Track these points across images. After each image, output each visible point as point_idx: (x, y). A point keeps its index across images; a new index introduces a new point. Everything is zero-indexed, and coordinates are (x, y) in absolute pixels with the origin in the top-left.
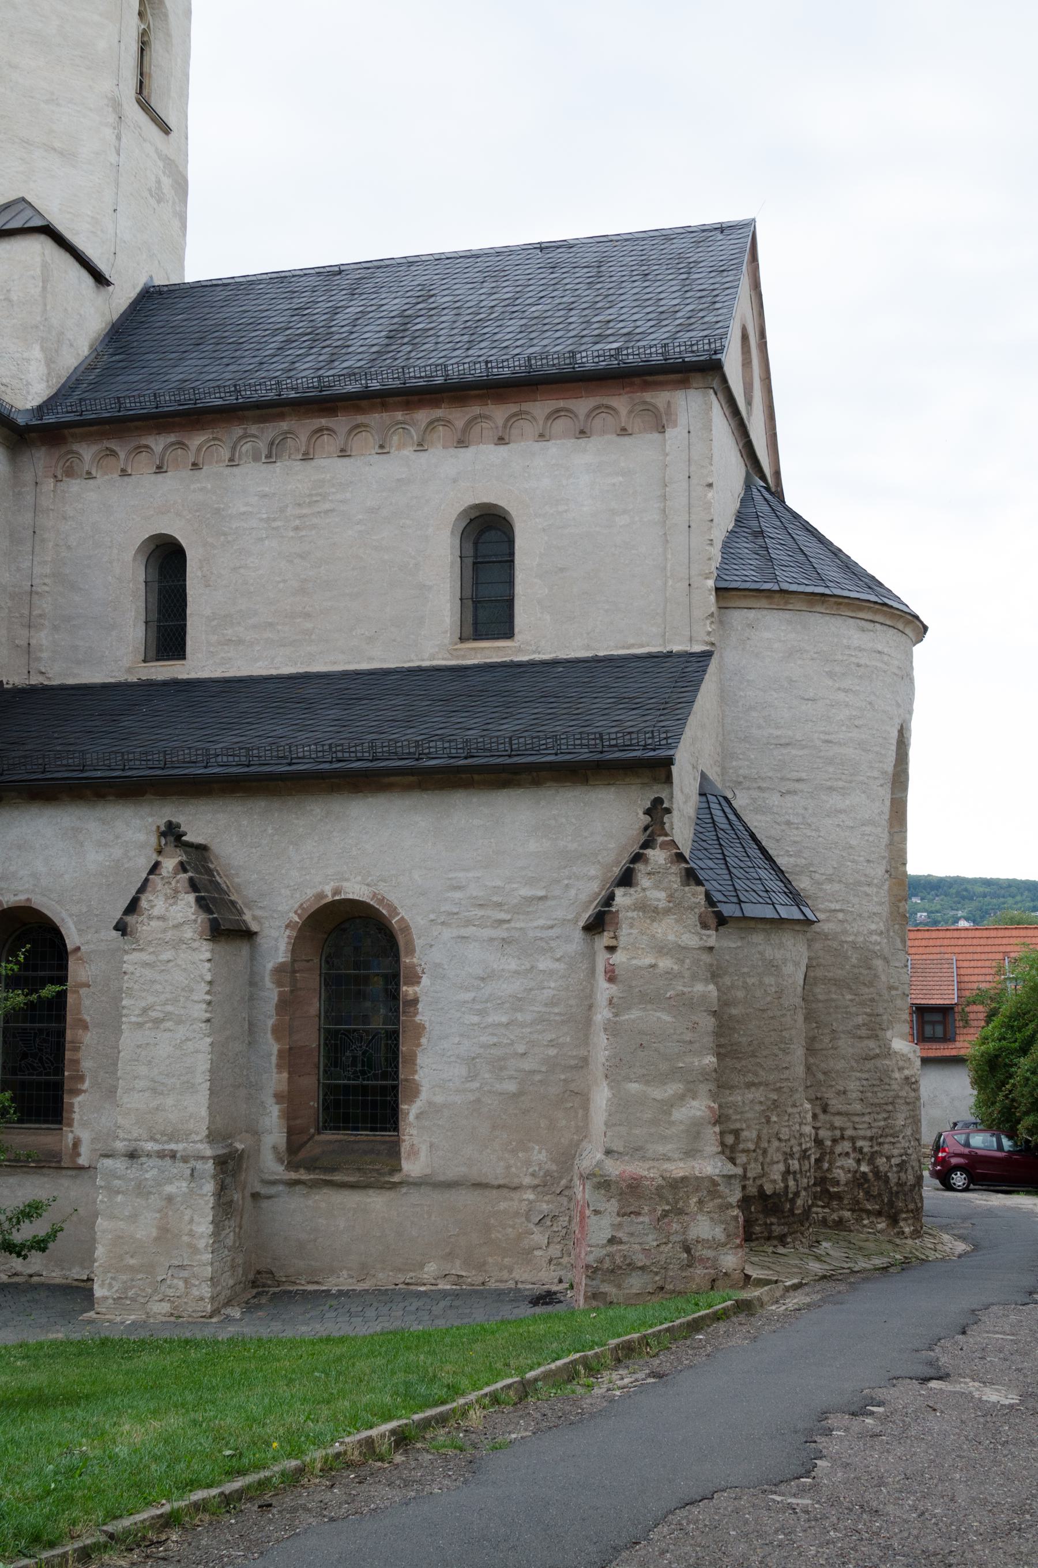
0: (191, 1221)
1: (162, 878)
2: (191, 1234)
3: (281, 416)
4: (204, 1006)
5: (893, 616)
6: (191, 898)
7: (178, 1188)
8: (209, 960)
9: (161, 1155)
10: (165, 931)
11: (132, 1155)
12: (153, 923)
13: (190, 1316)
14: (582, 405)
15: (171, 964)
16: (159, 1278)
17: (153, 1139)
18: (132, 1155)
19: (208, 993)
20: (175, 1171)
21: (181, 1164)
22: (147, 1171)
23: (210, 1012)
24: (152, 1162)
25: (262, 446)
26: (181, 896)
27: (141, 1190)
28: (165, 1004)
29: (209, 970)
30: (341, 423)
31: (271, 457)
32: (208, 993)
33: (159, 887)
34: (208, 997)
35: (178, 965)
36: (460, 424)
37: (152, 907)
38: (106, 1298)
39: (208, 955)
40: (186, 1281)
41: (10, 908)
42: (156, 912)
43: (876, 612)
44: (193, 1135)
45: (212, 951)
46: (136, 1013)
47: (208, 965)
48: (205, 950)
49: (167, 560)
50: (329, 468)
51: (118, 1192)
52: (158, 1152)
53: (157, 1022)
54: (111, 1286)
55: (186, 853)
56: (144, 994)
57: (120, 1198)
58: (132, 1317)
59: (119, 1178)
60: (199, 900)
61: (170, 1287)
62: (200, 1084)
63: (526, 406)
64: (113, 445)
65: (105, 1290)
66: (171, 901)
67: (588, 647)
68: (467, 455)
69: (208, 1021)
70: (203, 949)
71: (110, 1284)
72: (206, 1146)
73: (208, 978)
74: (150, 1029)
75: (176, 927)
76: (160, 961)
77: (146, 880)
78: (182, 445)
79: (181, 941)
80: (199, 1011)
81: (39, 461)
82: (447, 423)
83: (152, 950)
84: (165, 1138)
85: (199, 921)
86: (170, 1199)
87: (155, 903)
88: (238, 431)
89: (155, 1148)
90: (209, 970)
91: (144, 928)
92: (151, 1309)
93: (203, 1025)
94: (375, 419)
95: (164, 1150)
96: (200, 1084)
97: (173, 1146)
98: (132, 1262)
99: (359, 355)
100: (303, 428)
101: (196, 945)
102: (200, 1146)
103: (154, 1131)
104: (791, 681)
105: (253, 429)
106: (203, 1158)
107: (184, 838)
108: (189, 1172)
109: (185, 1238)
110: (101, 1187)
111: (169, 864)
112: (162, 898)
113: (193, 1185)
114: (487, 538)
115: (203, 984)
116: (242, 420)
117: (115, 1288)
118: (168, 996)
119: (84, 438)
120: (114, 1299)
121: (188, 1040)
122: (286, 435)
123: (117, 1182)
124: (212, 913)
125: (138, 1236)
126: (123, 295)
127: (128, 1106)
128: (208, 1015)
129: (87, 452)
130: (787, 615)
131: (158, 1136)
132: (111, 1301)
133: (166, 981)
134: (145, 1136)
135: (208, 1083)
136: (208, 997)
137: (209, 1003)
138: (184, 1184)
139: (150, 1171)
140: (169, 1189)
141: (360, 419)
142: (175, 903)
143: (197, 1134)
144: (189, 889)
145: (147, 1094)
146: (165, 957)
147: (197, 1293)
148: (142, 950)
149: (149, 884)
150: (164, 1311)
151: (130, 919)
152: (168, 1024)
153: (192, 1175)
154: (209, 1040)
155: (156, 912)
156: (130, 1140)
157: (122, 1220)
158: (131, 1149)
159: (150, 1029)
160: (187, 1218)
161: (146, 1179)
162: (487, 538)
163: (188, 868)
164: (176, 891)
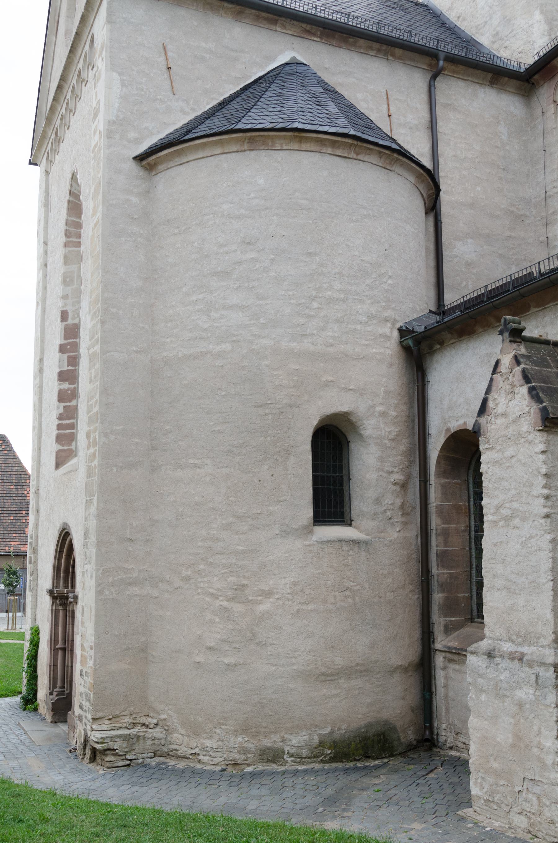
0: (539, 733)
1: (502, 375)
2: (540, 747)
4: (542, 501)
6: (524, 390)
7: (525, 693)
8: (543, 452)
9: (512, 657)
10: (507, 427)
11: (490, 655)
12: (499, 421)
13: (544, 839)
15: (514, 460)
16: (517, 789)
17: (510, 640)
18: (490, 655)
19: (545, 486)
20: (523, 675)
21: (527, 669)
22: (501, 673)
23: (551, 507)
24: (505, 663)
26: (516, 390)
27: (499, 693)
28: (512, 501)
29: (545, 462)
32: (545, 486)
33: (501, 384)
34: (545, 491)
35: (519, 460)
37: (497, 405)
38: (479, 797)
39: (542, 447)
40: (539, 797)
41: (455, 432)
42: (500, 409)
44: (542, 639)
45: (547, 442)
46: (492, 511)
47: (542, 457)
48: (539, 441)
51: (482, 691)
52: (510, 653)
53: (508, 519)
54: (482, 788)
55: (526, 348)
56: (496, 492)
57: (483, 697)
58: (497, 824)
59: (481, 676)
60: (531, 390)
61: (526, 800)
62: (544, 584)
65: (478, 789)
66: (510, 397)
69: (547, 516)
70: (537, 441)
71: (481, 784)
72: (552, 651)
73: (544, 471)
74: (503, 527)
75: (514, 421)
76: (506, 458)
77: (492, 380)
79: (520, 435)
80: (538, 507)
83: (498, 448)
84: (520, 640)
85: (532, 412)
86: (520, 705)
87: (499, 402)
89: (511, 650)
90: (545, 462)
91: (493, 427)
92: (513, 820)
93: (543, 521)
95: (516, 652)
96: (544, 584)
97: (525, 649)
98: (496, 765)
101: (531, 437)
102: (547, 651)
103: (511, 632)
106: (545, 664)
107: (524, 334)
108: (533, 678)
109: (535, 750)
110: (470, 684)
111: (507, 360)
112: (503, 395)
113: (538, 693)
115: (540, 478)
117: (485, 790)
118: (513, 492)
120: (485, 800)
121: (531, 537)
123: (480, 681)
124: (541, 402)
125: (498, 739)
127: (491, 604)
128: (547, 510)
131: (514, 637)
132: (483, 802)
133: (511, 478)
134: (505, 637)
135: (551, 583)
136: (545, 491)
137: (547, 497)
138: (531, 692)
139: (504, 672)
140: (520, 694)
142: (513, 398)
143: (545, 638)
144: (523, 381)
145: (504, 593)
146: (510, 452)
147: (548, 815)
148: (492, 448)
149: (494, 383)
150: (523, 826)
151: (483, 420)
152: (516, 522)
153: (537, 682)
154: (549, 537)
155: (500, 409)
156: (494, 639)
157: (486, 720)
158: (491, 648)
159: (503, 527)
160: (535, 728)
161: (501, 680)
163: (521, 360)
164: (513, 386)
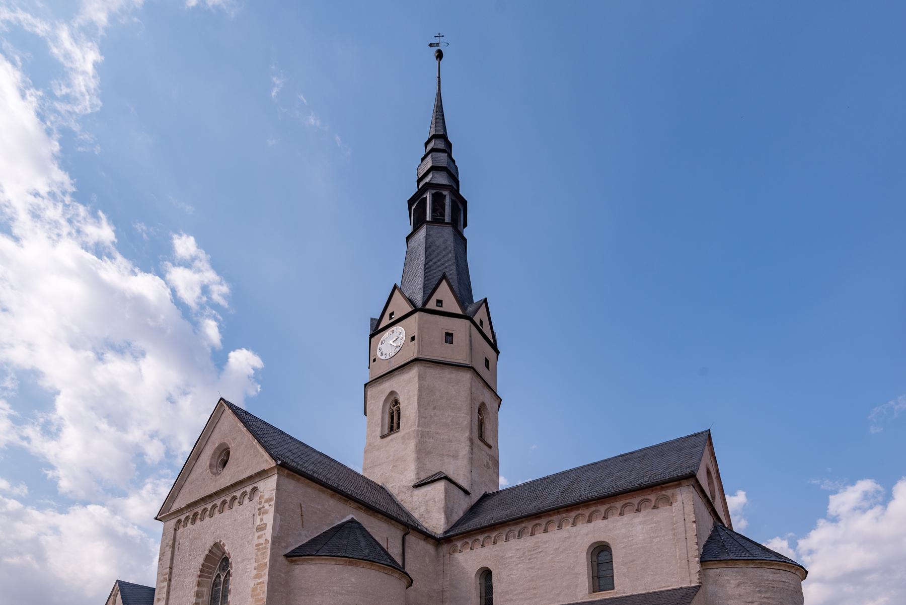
3: (522, 522)
5: (789, 567)
14: (636, 501)
25: (517, 533)
30: (543, 521)
31: (520, 536)
36: (587, 515)
43: (780, 565)
49: (486, 574)
50: (540, 537)
63: (613, 504)
64: (467, 540)
67: (645, 589)
68: (591, 525)
78: (489, 537)
81: (445, 548)
82: (582, 515)
88: (507, 529)
94: (555, 518)
99: (551, 499)
100: (529, 525)
104: (740, 595)
105: (513, 528)
114: (600, 554)
116: (509, 525)
119: (458, 539)
122: (524, 528)
126: (476, 497)
129: (459, 544)
130: (736, 569)
141: (550, 519)
162: (600, 554)
